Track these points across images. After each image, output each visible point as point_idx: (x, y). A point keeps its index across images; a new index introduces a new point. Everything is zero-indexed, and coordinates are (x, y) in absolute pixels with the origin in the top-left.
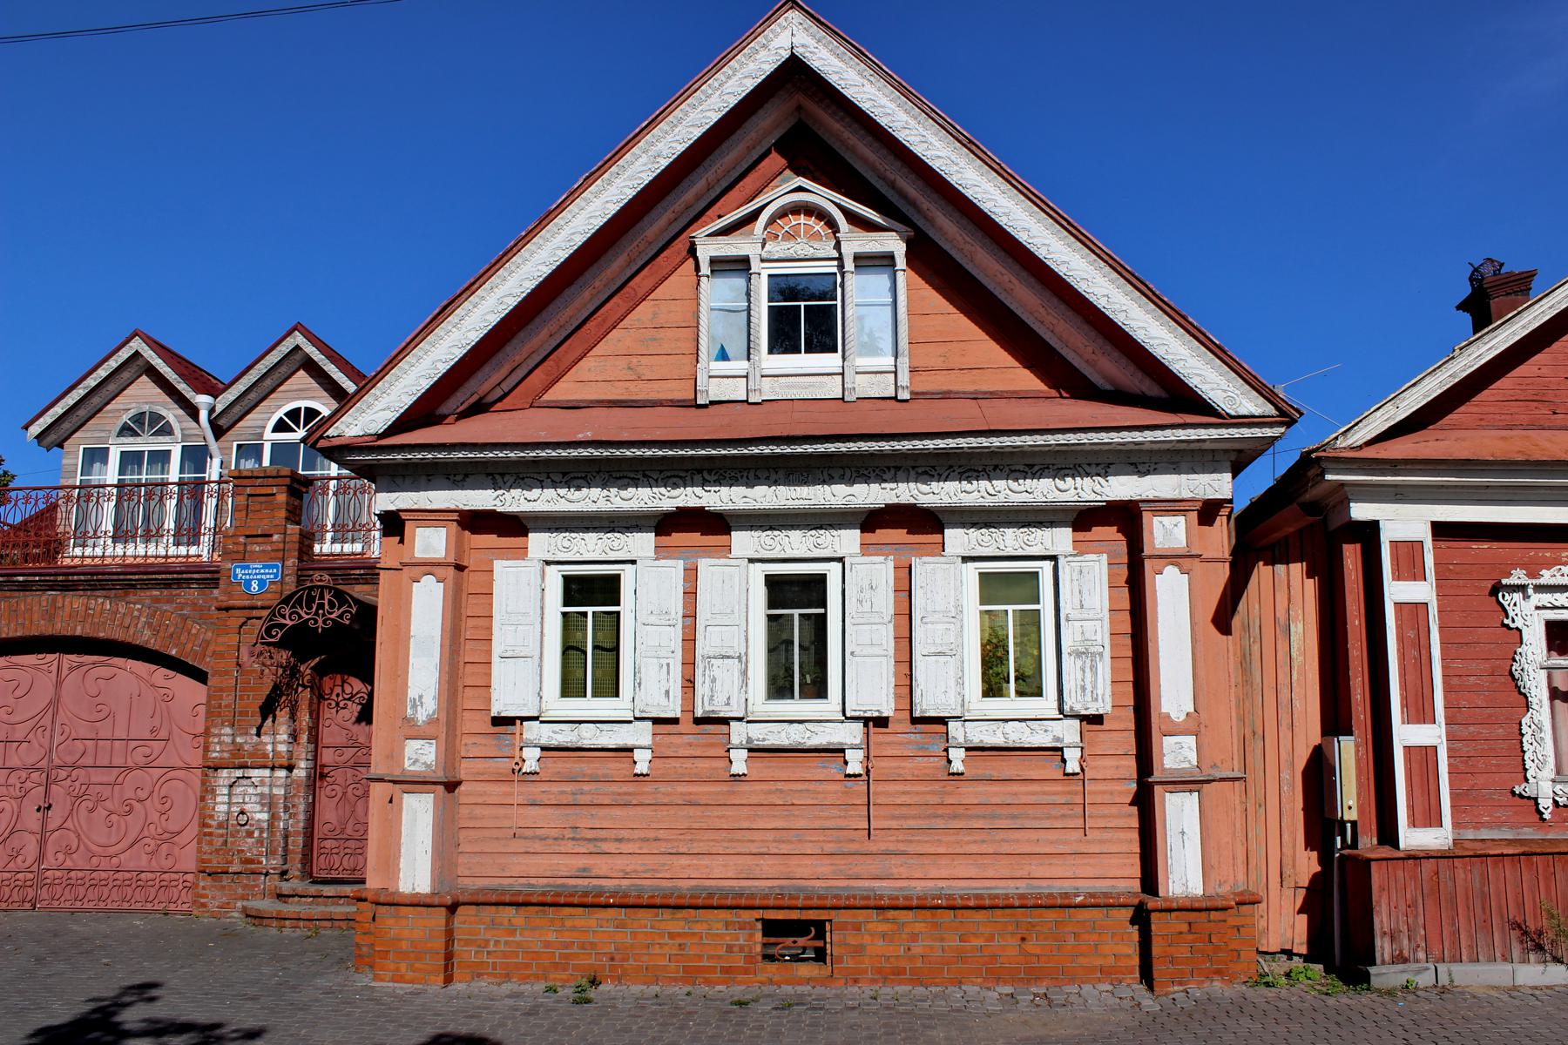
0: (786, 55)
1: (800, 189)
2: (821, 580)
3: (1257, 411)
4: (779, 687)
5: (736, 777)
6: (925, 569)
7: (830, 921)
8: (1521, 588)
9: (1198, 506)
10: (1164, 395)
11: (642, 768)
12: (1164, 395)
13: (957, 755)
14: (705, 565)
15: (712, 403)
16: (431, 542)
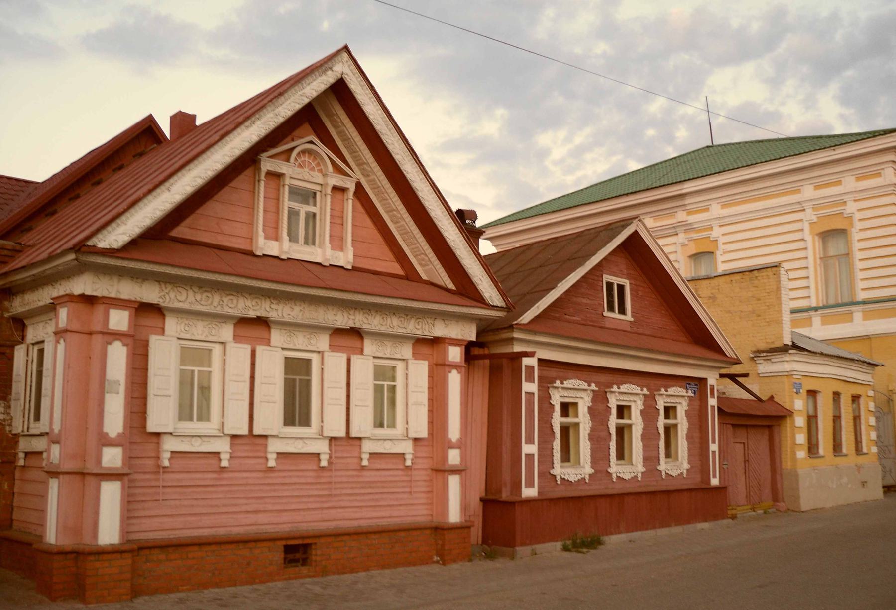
0: (340, 76)
1: (311, 142)
2: (308, 362)
3: (499, 305)
4: (289, 420)
5: (271, 469)
6: (356, 360)
7: (315, 543)
8: (557, 388)
9: (465, 343)
10: (454, 288)
11: (225, 463)
12: (454, 288)
13: (365, 456)
14: (260, 349)
15: (264, 255)
16: (119, 320)
